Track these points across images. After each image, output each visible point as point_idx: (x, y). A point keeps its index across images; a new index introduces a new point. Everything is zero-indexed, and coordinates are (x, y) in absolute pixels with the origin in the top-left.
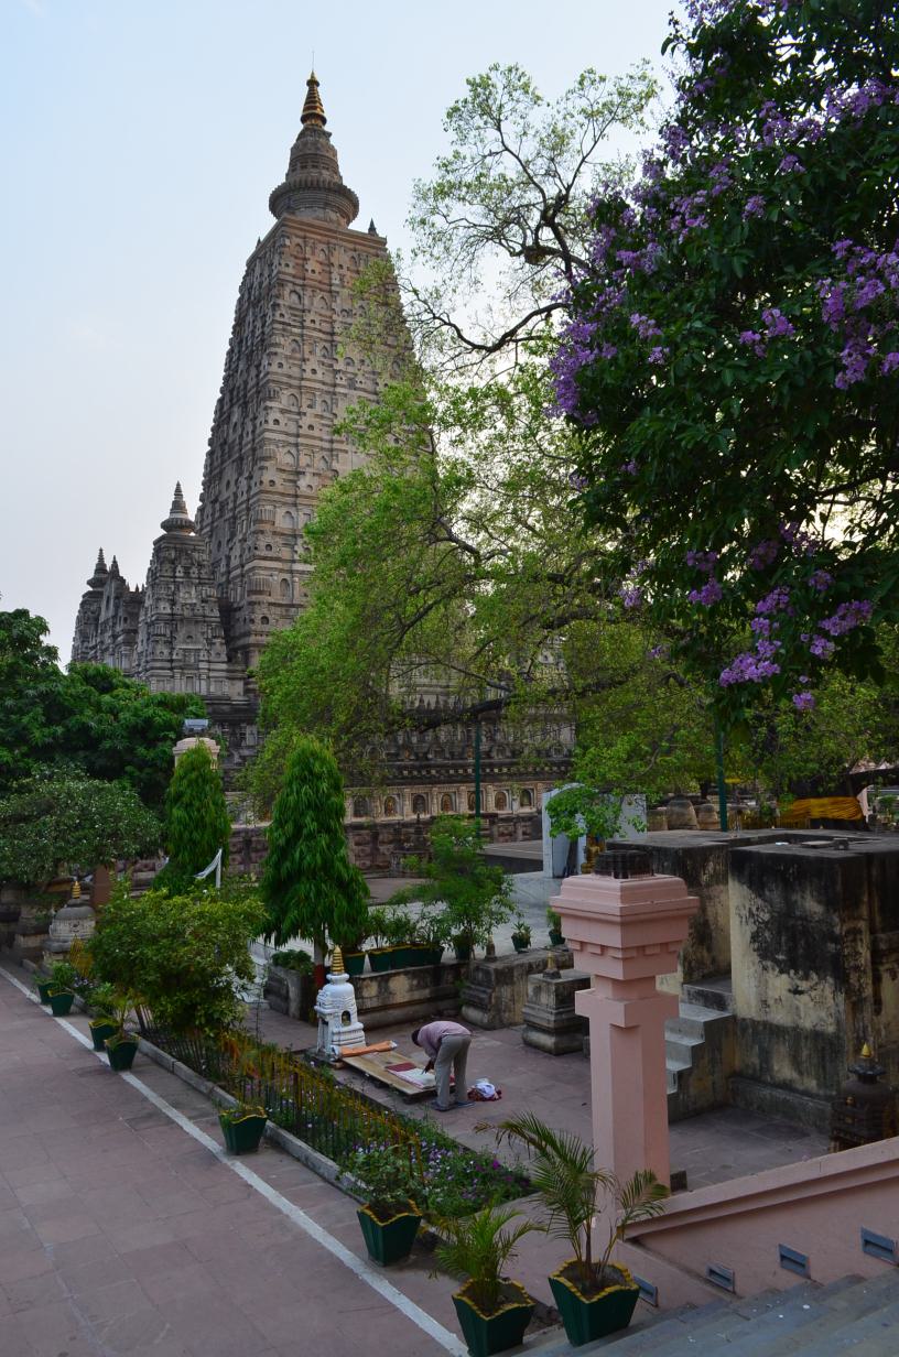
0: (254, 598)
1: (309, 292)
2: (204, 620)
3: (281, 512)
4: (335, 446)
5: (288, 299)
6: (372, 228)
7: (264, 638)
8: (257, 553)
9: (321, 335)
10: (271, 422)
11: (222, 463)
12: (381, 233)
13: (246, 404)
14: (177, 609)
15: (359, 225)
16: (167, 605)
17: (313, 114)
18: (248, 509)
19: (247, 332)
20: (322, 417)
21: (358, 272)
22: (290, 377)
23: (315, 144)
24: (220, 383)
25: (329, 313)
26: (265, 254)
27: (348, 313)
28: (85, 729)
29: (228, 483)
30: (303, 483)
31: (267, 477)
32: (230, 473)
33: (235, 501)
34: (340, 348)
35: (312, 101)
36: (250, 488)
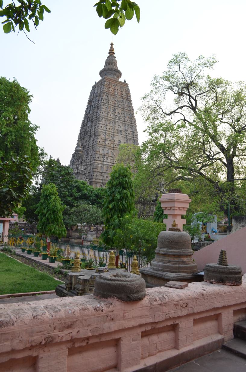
0: (94, 170)
1: (110, 96)
2: (84, 174)
3: (101, 149)
4: (115, 134)
5: (105, 97)
6: (125, 81)
7: (96, 180)
8: (96, 159)
9: (112, 106)
10: (100, 127)
11: (84, 136)
12: (127, 82)
13: (92, 122)
14: (79, 171)
15: (121, 80)
16: (76, 170)
17: (111, 52)
18: (93, 148)
19: (93, 104)
20: (112, 126)
21: (121, 92)
22: (105, 116)
23: (112, 59)
24: (84, 116)
25: (114, 101)
26: (97, 86)
27: (119, 101)
28: (85, 194)
29: (86, 141)
30: (107, 142)
31: (99, 140)
32: (87, 138)
33: (88, 146)
34: (117, 110)
35: (112, 49)
36: (93, 142)
